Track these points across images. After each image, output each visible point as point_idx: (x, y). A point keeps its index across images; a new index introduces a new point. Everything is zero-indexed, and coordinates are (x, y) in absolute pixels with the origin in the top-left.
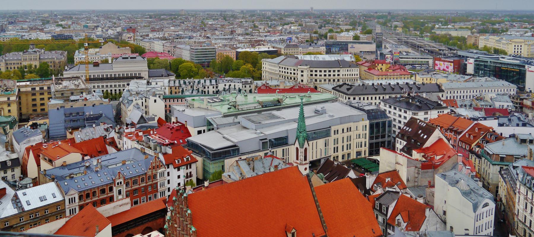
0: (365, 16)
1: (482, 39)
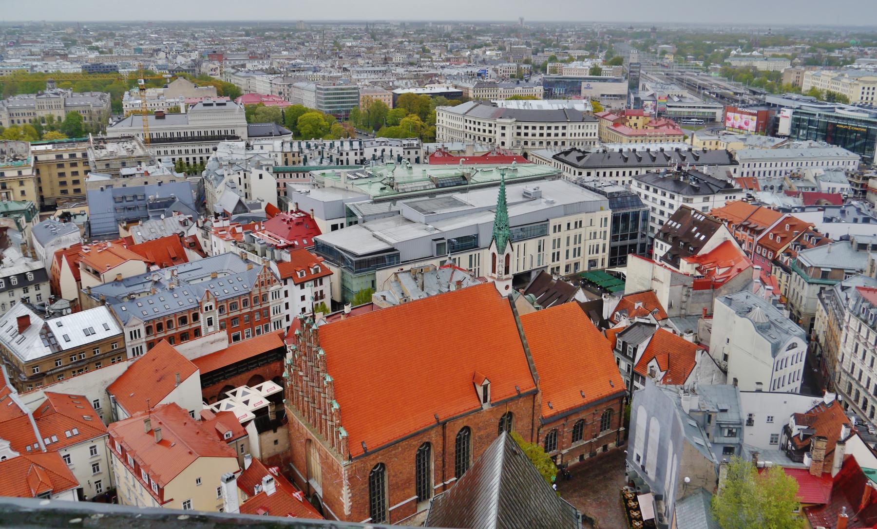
0: (610, 33)
1: (808, 77)
